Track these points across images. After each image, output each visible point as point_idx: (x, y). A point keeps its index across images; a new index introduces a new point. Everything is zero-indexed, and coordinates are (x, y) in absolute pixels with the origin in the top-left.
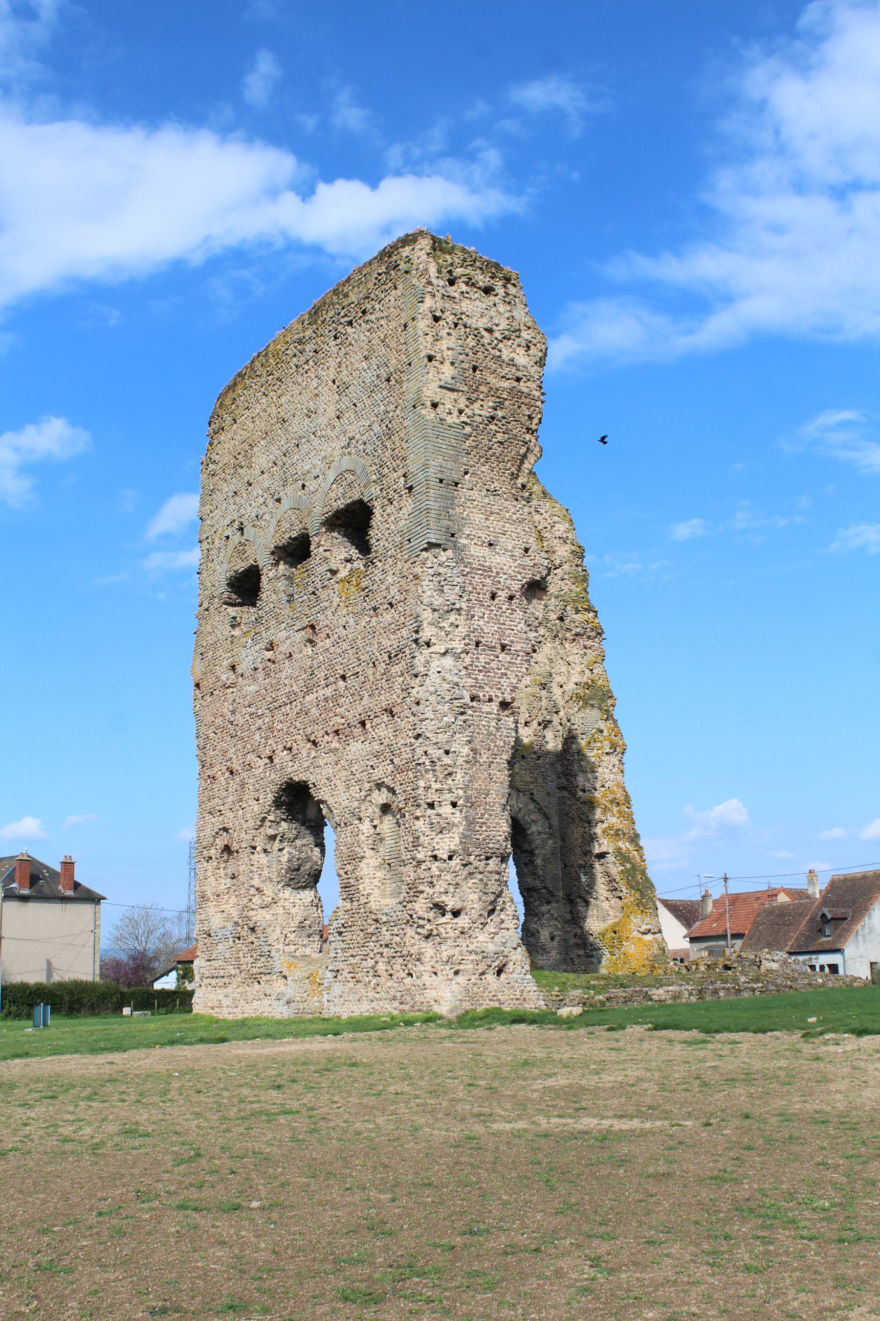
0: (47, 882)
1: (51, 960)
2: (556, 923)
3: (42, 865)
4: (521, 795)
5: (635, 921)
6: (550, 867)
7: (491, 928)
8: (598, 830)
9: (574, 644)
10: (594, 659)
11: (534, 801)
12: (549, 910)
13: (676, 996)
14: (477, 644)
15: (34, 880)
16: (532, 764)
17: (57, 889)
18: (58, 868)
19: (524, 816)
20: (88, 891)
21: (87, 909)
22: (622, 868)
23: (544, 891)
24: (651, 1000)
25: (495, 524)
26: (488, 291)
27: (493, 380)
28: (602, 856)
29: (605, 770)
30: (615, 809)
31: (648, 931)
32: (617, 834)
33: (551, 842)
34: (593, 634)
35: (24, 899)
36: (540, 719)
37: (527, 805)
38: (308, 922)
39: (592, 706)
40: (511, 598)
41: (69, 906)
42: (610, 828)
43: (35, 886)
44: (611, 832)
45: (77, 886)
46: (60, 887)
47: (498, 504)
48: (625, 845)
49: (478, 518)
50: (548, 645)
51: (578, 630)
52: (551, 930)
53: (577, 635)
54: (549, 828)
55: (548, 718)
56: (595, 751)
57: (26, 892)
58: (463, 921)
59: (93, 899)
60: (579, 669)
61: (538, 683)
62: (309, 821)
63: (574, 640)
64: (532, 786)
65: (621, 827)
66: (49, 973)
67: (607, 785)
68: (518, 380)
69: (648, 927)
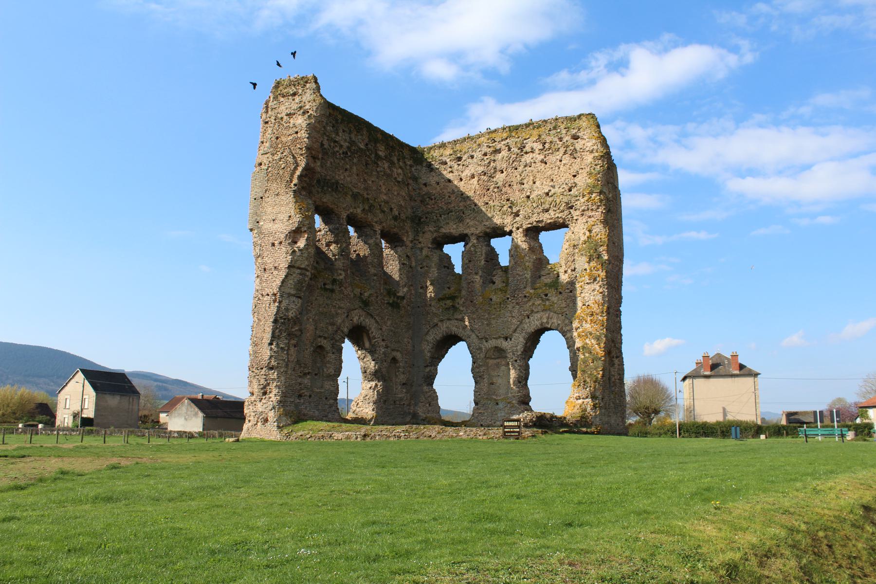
7: (263, 401)
14: (265, 269)
20: (750, 370)
21: (750, 380)
25: (277, 209)
26: (294, 94)
27: (284, 139)
30: (589, 319)
34: (594, 207)
40: (281, 243)
41: (736, 379)
45: (742, 367)
47: (278, 199)
49: (269, 210)
53: (583, 211)
57: (708, 373)
58: (253, 398)
59: (756, 375)
63: (582, 215)
65: (591, 330)
66: (725, 414)
68: (297, 133)
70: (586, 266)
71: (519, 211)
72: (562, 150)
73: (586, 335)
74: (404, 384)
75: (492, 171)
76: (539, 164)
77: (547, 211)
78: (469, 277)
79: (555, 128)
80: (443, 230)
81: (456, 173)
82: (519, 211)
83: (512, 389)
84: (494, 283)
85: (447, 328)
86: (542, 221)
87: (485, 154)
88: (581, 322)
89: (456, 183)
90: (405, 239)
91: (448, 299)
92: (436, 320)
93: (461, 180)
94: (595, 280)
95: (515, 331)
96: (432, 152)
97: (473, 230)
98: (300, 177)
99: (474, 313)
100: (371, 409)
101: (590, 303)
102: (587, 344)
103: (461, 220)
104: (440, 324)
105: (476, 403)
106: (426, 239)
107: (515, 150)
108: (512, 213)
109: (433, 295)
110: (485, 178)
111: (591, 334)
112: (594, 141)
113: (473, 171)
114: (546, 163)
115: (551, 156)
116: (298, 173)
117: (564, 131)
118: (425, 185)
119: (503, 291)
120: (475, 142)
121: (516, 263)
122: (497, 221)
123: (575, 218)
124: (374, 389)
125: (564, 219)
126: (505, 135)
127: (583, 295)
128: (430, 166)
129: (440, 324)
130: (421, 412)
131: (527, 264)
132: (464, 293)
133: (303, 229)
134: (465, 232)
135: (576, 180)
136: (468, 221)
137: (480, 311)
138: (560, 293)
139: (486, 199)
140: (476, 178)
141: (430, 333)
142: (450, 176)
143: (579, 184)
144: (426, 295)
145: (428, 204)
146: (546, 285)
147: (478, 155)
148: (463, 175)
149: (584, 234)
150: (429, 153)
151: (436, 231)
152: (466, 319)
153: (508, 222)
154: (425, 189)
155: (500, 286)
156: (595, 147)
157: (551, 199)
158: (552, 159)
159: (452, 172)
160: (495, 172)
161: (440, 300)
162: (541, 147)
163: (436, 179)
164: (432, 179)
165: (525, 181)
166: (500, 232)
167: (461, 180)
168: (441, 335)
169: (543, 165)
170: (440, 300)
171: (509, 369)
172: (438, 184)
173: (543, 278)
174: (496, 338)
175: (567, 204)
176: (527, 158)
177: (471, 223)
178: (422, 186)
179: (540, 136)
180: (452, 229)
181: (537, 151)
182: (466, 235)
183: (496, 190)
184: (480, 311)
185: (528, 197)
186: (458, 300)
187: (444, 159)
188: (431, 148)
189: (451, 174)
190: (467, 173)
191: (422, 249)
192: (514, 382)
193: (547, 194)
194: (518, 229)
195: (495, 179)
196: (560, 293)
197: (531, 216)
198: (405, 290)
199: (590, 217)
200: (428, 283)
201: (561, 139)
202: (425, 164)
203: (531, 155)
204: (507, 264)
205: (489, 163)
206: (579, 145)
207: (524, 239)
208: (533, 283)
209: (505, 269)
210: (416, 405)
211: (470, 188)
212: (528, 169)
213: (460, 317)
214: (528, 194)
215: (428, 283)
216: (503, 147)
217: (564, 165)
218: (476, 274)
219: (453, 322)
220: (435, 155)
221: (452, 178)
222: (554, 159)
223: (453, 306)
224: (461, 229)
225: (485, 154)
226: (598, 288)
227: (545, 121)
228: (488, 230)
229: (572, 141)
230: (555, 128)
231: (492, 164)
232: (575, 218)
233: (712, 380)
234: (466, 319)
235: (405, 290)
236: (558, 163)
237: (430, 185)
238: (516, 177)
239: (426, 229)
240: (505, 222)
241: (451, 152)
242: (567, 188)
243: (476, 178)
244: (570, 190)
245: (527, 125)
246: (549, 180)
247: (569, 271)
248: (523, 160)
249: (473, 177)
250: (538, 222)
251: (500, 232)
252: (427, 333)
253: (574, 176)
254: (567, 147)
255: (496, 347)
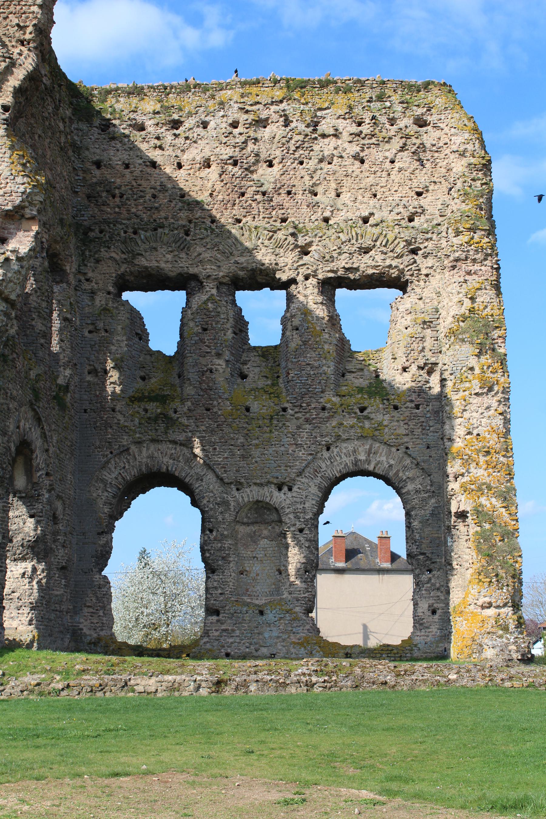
0: (367, 556)
1: (367, 625)
2: (439, 594)
3: (366, 540)
4: (394, 449)
5: (472, 591)
6: (428, 530)
8: (453, 486)
9: (455, 271)
10: (478, 286)
11: (410, 455)
12: (430, 579)
13: (173, 688)
15: (350, 554)
16: (407, 414)
17: (374, 562)
18: (376, 541)
19: (397, 473)
22: (479, 529)
23: (421, 557)
24: (133, 691)
28: (462, 515)
29: (474, 414)
30: (482, 460)
31: (490, 605)
32: (481, 488)
33: (433, 501)
34: (479, 256)
35: (340, 571)
36: (421, 362)
37: (401, 460)
38: (16, 595)
39: (463, 340)
41: (386, 577)
42: (472, 482)
43: (353, 560)
44: (473, 487)
46: (378, 560)
48: (488, 502)
50: (438, 277)
51: (457, 255)
52: (431, 602)
53: (457, 260)
54: (431, 485)
55: (433, 360)
56: (461, 394)
57: (341, 565)
60: (456, 300)
61: (419, 321)
62: (20, 492)
63: (454, 267)
64: (406, 439)
65: (487, 480)
66: (366, 637)
67: (475, 432)
69: (487, 599)
70: (473, 362)
71: (310, 244)
72: (397, 143)
73: (480, 489)
74: (63, 568)
75: (252, 159)
76: (348, 161)
77: (367, 251)
78: (203, 361)
79: (380, 98)
80: (143, 262)
81: (169, 151)
82: (310, 244)
83: (292, 584)
84: (244, 376)
85: (151, 457)
86: (357, 269)
87: (235, 125)
88: (466, 462)
89: (168, 170)
90: (68, 268)
91: (151, 399)
92: (125, 440)
93: (180, 166)
94: (490, 389)
95: (300, 474)
96: (111, 100)
97: (209, 269)
98: (18, 92)
99: (212, 432)
100: (25, 619)
101: (480, 430)
102: (481, 505)
103: (185, 247)
104: (133, 449)
105: (211, 611)
106: (103, 275)
107: (302, 127)
108: (297, 246)
109: (118, 389)
110: (236, 170)
111: (489, 488)
112: (467, 136)
113: (207, 153)
114: (362, 162)
115: (373, 150)
116: (15, 80)
117: (399, 108)
118: (98, 164)
119: (272, 393)
120: (213, 97)
121: (305, 343)
122: (264, 257)
123: (424, 271)
124: (31, 578)
125: (402, 272)
126: (278, 94)
127: (466, 415)
128: (106, 125)
129: (133, 449)
130: (85, 626)
131: (326, 347)
132: (189, 390)
133: (28, 212)
134: (192, 271)
135: (424, 201)
136: (199, 249)
137: (226, 429)
138: (396, 408)
139: (237, 211)
140: (215, 169)
141: (111, 466)
142: (155, 155)
143: (430, 210)
144: (104, 389)
145: (105, 204)
146: (360, 390)
147: (218, 123)
148: (185, 158)
149: (461, 302)
150: (104, 101)
151: (125, 261)
152: (197, 442)
153: (286, 264)
154: (97, 172)
155: (261, 383)
156: (470, 147)
157: (376, 231)
158: (374, 155)
159: (161, 148)
160: (257, 162)
161: (133, 400)
162: (354, 129)
163: (124, 156)
164: (117, 157)
165: (320, 190)
166: (262, 278)
167: (180, 166)
168: (135, 472)
169: (357, 163)
170: (133, 400)
171: (287, 547)
172: (127, 166)
173: (349, 376)
174: (261, 485)
175: (409, 243)
176: (327, 146)
177: (207, 255)
178: (88, 165)
179: (350, 108)
180: (163, 261)
181: (345, 136)
182: (195, 277)
183: (259, 197)
184: (226, 429)
185: (326, 220)
186: (176, 404)
187: (140, 118)
188: (109, 92)
189: (158, 152)
190: (194, 154)
191: (93, 293)
192: (298, 570)
193: (365, 220)
194: (307, 278)
195: (255, 176)
196: (396, 408)
197: (331, 254)
198: (68, 372)
199: (469, 273)
200: (110, 364)
201: (392, 121)
202: (97, 122)
203: (333, 142)
204: (275, 340)
205: (245, 142)
206: (429, 137)
207: (320, 299)
208: (338, 385)
209: (265, 353)
210: (76, 611)
211: (202, 185)
212: (324, 165)
213: (181, 437)
214: (327, 214)
215: (110, 364)
216: (275, 117)
217: (400, 170)
218: (219, 355)
219: (163, 447)
220: (118, 107)
221: (159, 160)
222: (380, 156)
223: (166, 416)
224: (185, 265)
225: (235, 125)
226: (495, 405)
227: (362, 83)
228: (241, 273)
229: (416, 128)
230: (380, 98)
231: (251, 146)
232: (424, 271)
233: (348, 578)
234: (197, 442)
235: (68, 372)
236: (388, 165)
237: (111, 167)
238: (301, 179)
239: (104, 254)
240: (281, 262)
241: (158, 107)
242: (406, 214)
243: (215, 169)
244: (411, 220)
245: (324, 84)
246: (368, 195)
247: (413, 368)
248: (316, 148)
249: (207, 164)
250: (347, 270)
251: (262, 278)
252: (104, 466)
253: (419, 194)
254: (408, 137)
255: (258, 501)
